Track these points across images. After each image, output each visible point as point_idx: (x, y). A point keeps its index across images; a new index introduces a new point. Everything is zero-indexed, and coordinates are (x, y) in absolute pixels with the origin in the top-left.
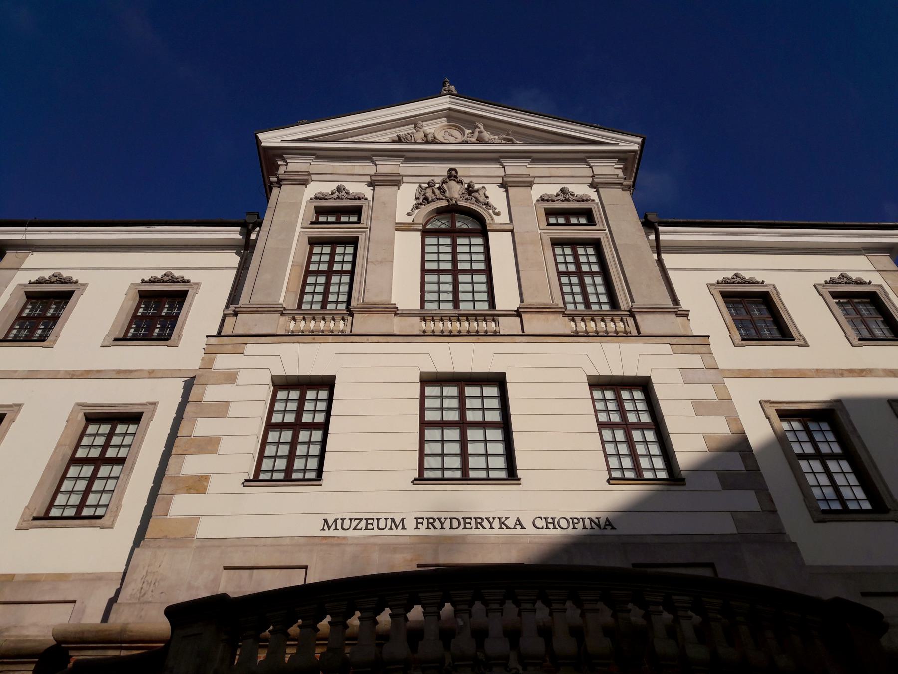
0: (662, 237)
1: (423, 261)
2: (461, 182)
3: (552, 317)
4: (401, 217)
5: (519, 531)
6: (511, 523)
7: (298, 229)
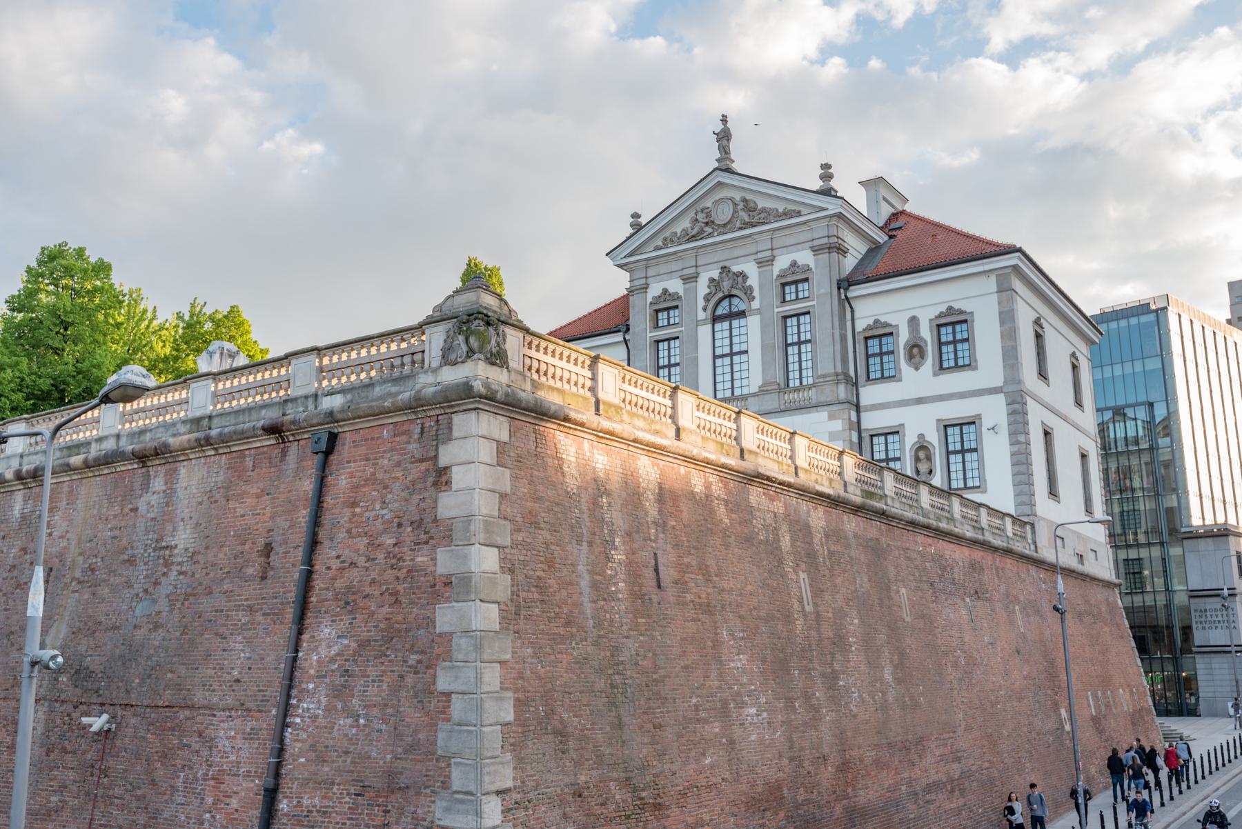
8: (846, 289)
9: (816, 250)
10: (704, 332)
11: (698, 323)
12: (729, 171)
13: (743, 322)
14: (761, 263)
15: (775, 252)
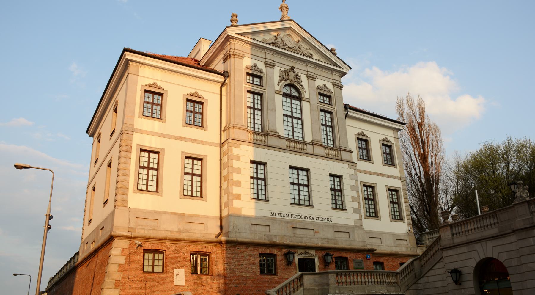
0: (349, 114)
2: (294, 73)
3: (321, 147)
4: (278, 88)
5: (313, 220)
6: (311, 218)
9: (334, 85)
10: (279, 98)
13: (298, 103)
14: (308, 77)
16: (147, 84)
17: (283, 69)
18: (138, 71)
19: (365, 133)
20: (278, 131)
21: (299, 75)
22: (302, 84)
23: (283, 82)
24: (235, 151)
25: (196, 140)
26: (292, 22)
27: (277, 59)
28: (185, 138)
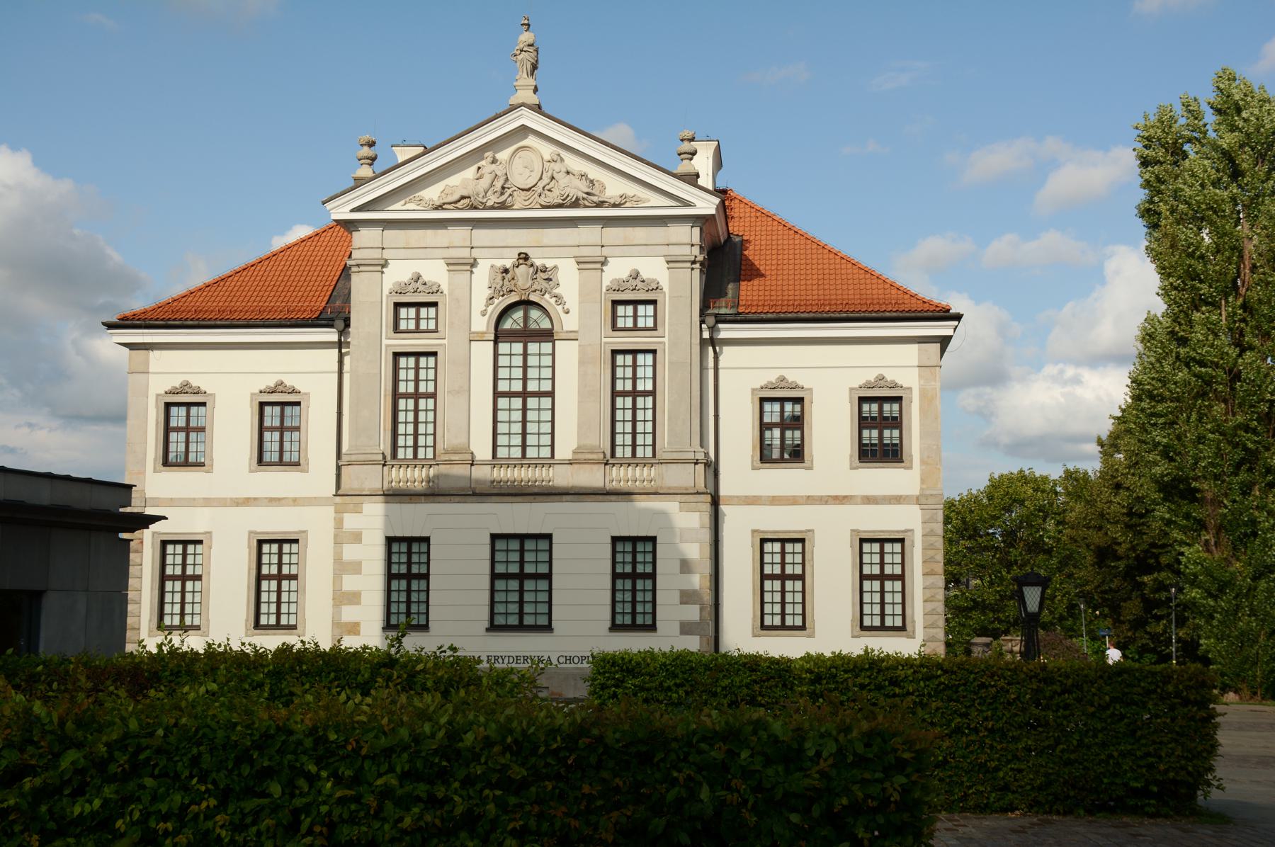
1: (496, 379)
3: (596, 467)
7: (385, 342)
8: (712, 329)
11: (475, 338)
12: (538, 109)
13: (546, 347)
15: (606, 251)
16: (168, 388)
17: (499, 263)
18: (147, 363)
19: (791, 377)
20: (472, 448)
21: (549, 264)
22: (556, 291)
23: (496, 301)
24: (351, 522)
25: (279, 499)
26: (524, 110)
27: (482, 236)
28: (255, 499)
